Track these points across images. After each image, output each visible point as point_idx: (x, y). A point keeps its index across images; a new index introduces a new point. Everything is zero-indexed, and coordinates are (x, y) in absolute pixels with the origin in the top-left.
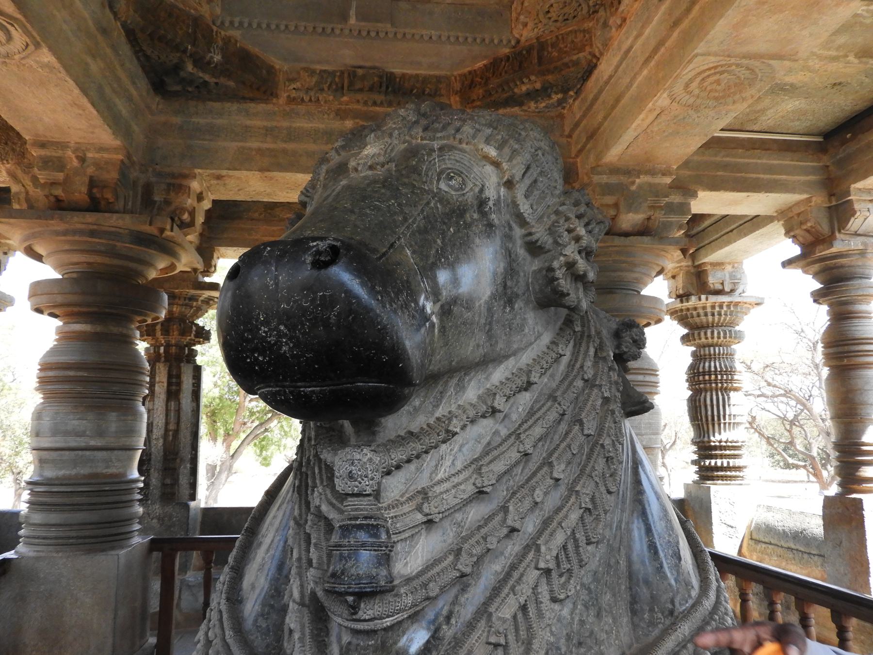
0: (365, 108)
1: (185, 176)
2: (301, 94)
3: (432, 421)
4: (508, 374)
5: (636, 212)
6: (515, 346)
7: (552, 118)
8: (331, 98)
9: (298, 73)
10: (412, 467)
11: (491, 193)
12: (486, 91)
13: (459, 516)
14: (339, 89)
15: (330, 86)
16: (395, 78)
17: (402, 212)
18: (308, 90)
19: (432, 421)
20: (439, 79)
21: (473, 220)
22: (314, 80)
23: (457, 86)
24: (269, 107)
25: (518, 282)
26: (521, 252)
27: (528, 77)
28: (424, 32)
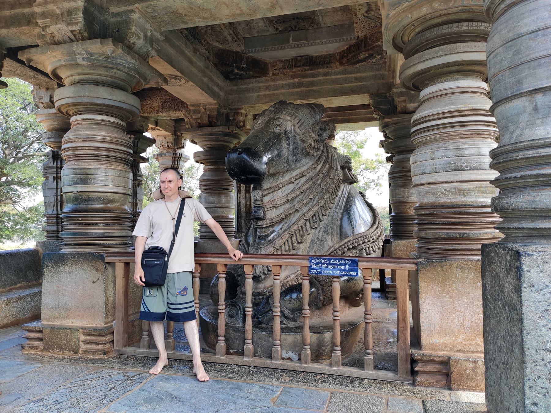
0: (302, 73)
1: (239, 109)
2: (277, 71)
3: (276, 185)
4: (298, 173)
5: (414, 103)
6: (298, 166)
7: (381, 64)
8: (289, 71)
9: (276, 63)
10: (271, 195)
11: (289, 129)
12: (347, 60)
13: (284, 207)
14: (291, 67)
15: (288, 66)
16: (313, 58)
17: (262, 138)
18: (280, 69)
19: (276, 185)
20: (330, 56)
21: (283, 137)
22: (282, 64)
23: (338, 58)
24: (266, 78)
25: (298, 150)
26: (299, 142)
27: (361, 53)
28: (319, 41)
